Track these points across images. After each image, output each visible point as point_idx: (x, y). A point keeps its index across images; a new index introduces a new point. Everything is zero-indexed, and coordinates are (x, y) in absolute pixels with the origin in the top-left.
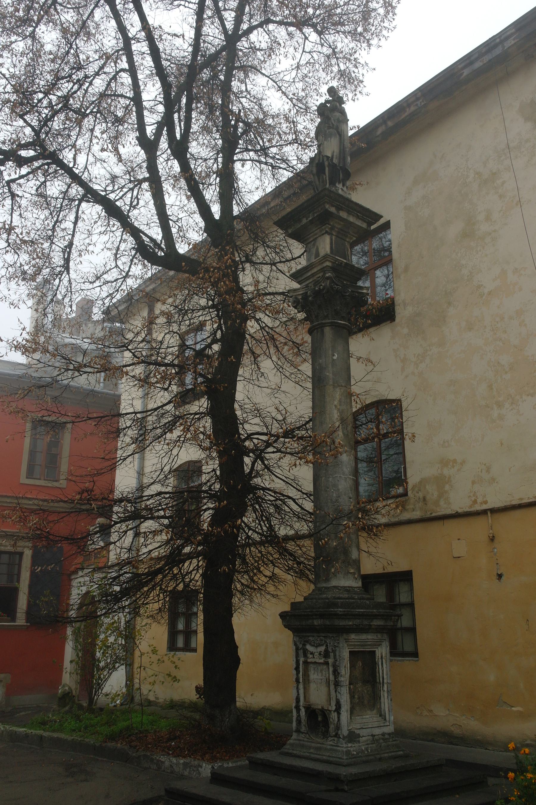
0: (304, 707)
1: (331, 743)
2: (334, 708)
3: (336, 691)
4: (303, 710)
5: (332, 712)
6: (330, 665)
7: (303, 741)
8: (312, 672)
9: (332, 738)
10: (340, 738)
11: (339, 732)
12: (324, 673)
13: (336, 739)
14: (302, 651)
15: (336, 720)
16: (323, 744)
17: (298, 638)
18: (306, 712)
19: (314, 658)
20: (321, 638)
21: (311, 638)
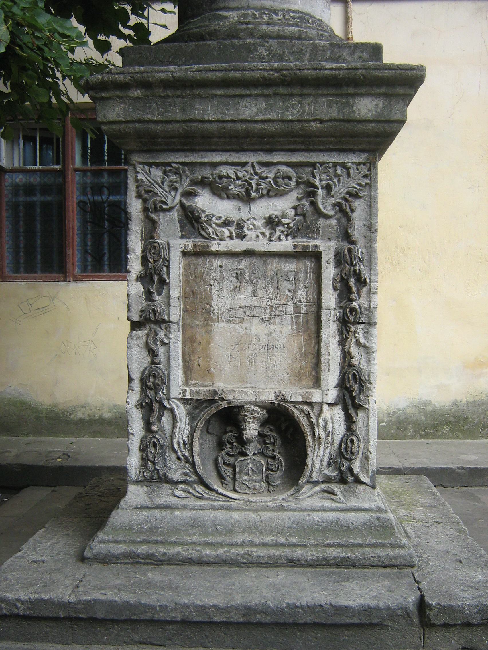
0: (186, 401)
1: (317, 502)
2: (332, 395)
3: (343, 342)
4: (181, 411)
5: (325, 407)
6: (324, 258)
7: (185, 507)
8: (228, 286)
9: (318, 488)
10: (358, 481)
11: (357, 467)
12: (286, 286)
13: (336, 488)
14: (175, 215)
15: (340, 430)
16: (282, 508)
17: (157, 173)
18: (192, 417)
19: (242, 237)
20: (284, 168)
21: (225, 170)
